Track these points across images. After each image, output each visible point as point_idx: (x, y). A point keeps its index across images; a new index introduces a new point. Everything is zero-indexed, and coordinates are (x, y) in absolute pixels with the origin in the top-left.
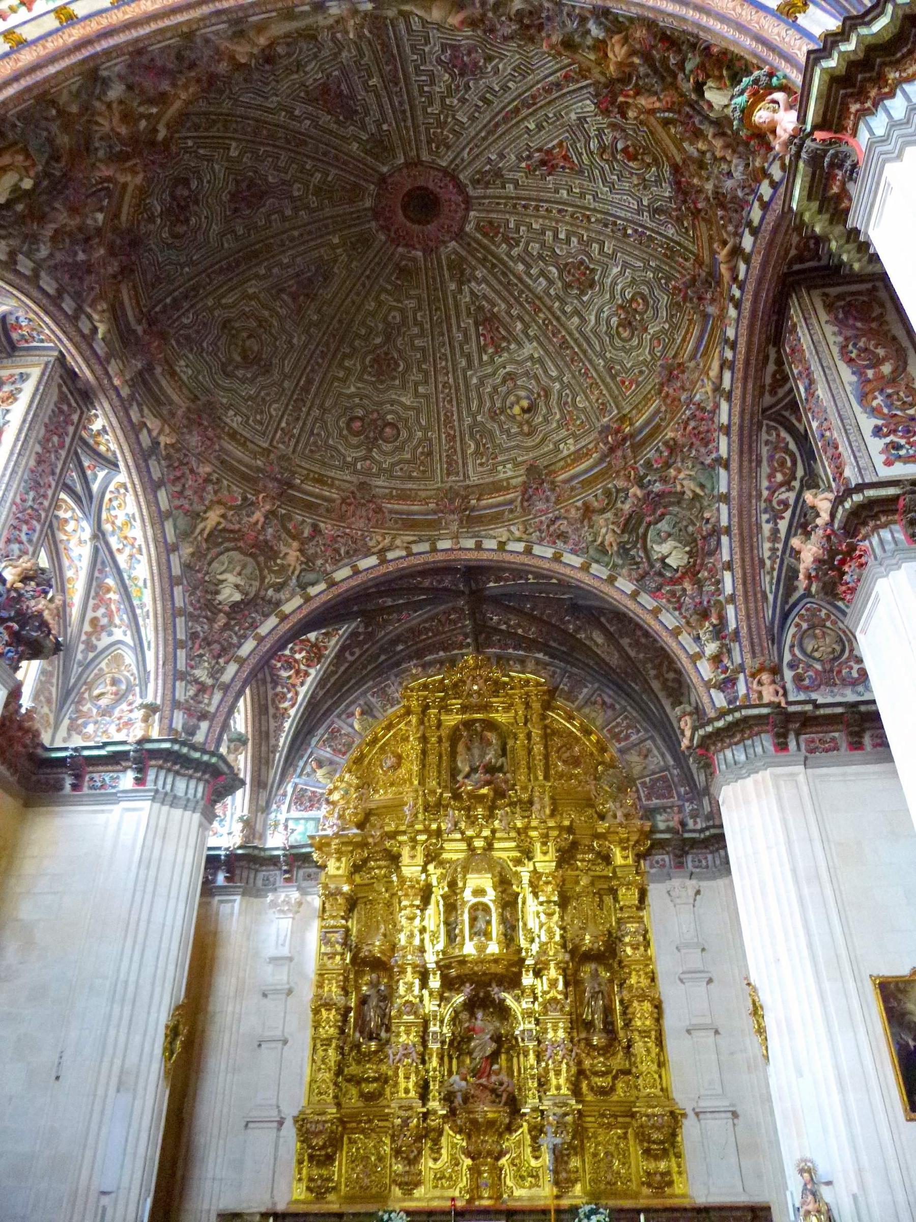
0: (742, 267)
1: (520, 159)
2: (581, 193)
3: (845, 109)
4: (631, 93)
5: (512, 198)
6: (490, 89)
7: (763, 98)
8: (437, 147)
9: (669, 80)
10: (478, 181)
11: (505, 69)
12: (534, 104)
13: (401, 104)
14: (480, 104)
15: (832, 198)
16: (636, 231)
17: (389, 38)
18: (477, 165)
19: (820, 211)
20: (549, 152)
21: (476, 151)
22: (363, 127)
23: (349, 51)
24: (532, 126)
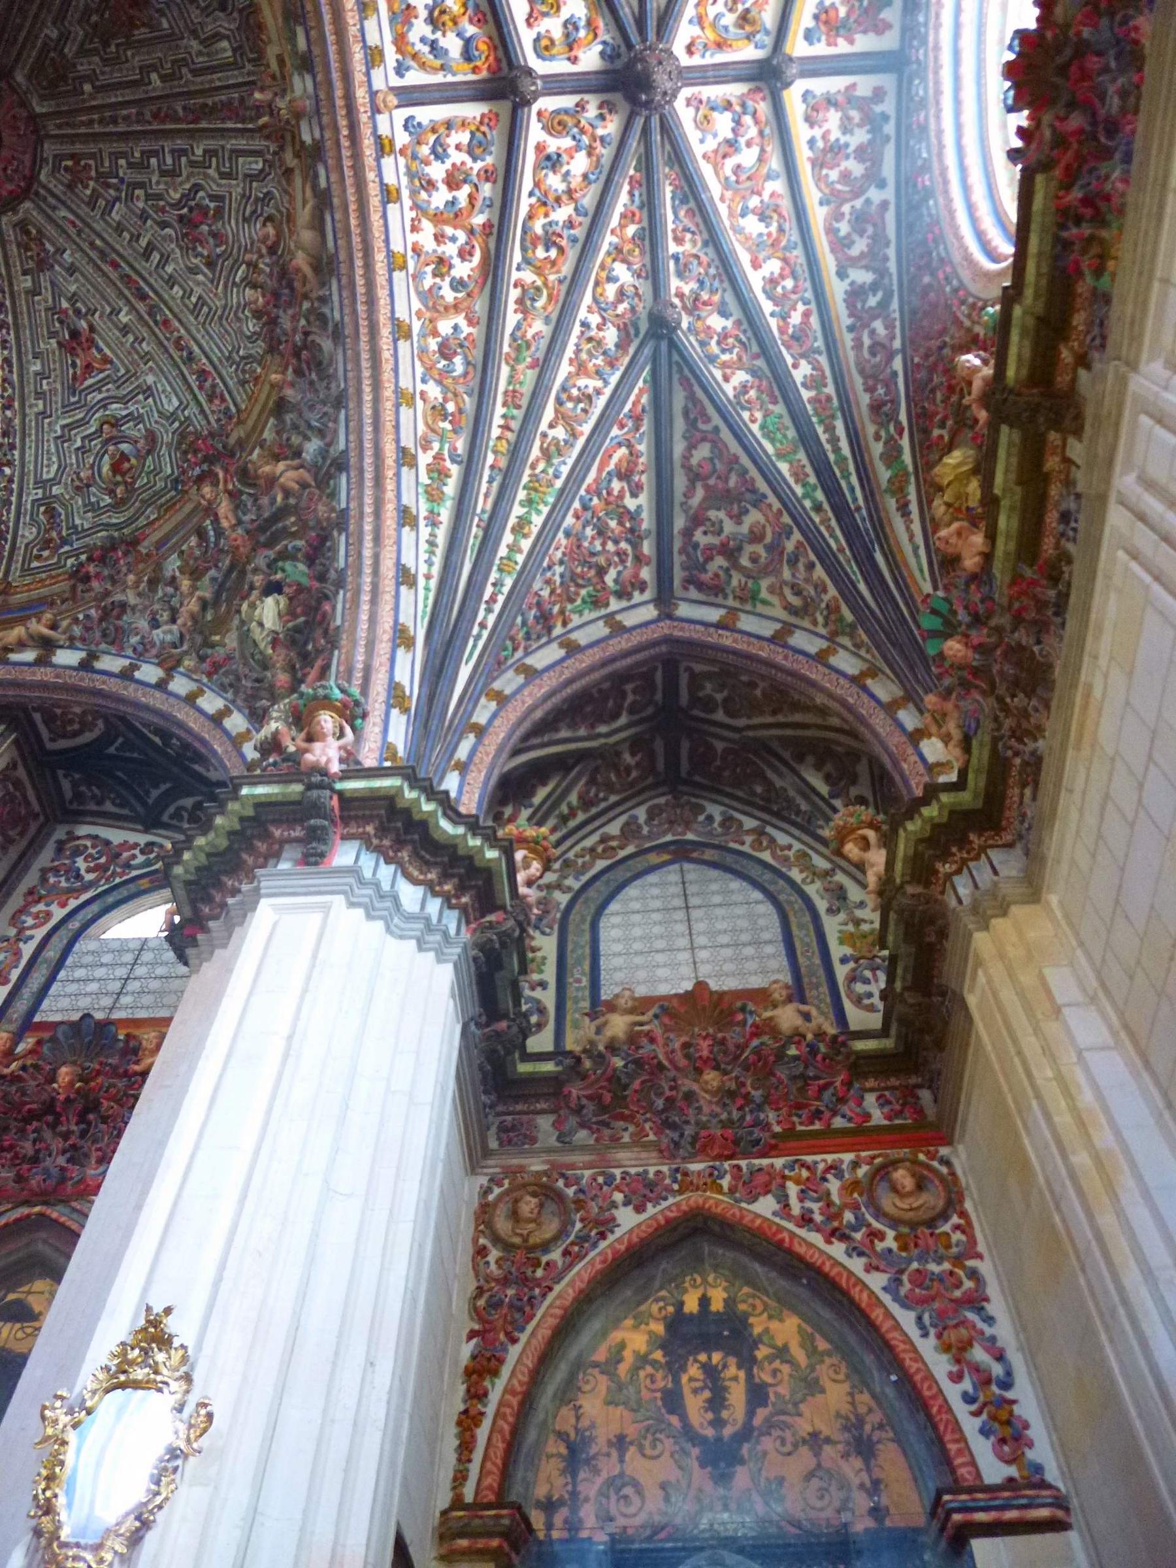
0: (29, 656)
1: (73, 299)
2: (44, 393)
3: (367, 820)
4: (230, 487)
5: (11, 285)
6: (165, 259)
7: (342, 715)
8: (66, 169)
9: (262, 539)
10: (28, 233)
11: (198, 284)
12: (156, 322)
13: (126, 118)
14: (143, 242)
15: (266, 830)
16: (11, 481)
17: (223, 120)
18: (50, 230)
19: (242, 819)
20: (91, 342)
21: (72, 231)
22: (83, 52)
23: (200, 53)
24: (124, 318)
